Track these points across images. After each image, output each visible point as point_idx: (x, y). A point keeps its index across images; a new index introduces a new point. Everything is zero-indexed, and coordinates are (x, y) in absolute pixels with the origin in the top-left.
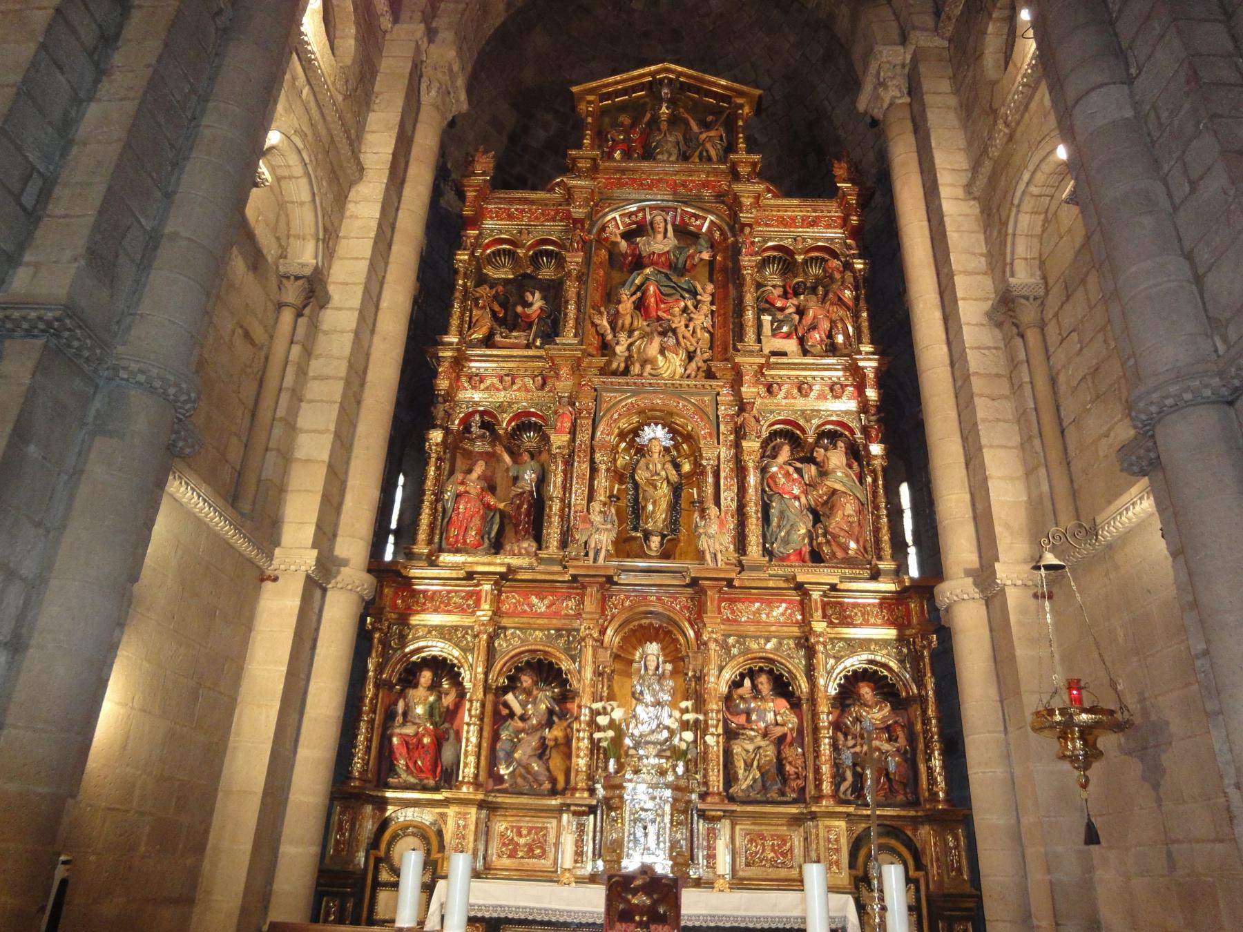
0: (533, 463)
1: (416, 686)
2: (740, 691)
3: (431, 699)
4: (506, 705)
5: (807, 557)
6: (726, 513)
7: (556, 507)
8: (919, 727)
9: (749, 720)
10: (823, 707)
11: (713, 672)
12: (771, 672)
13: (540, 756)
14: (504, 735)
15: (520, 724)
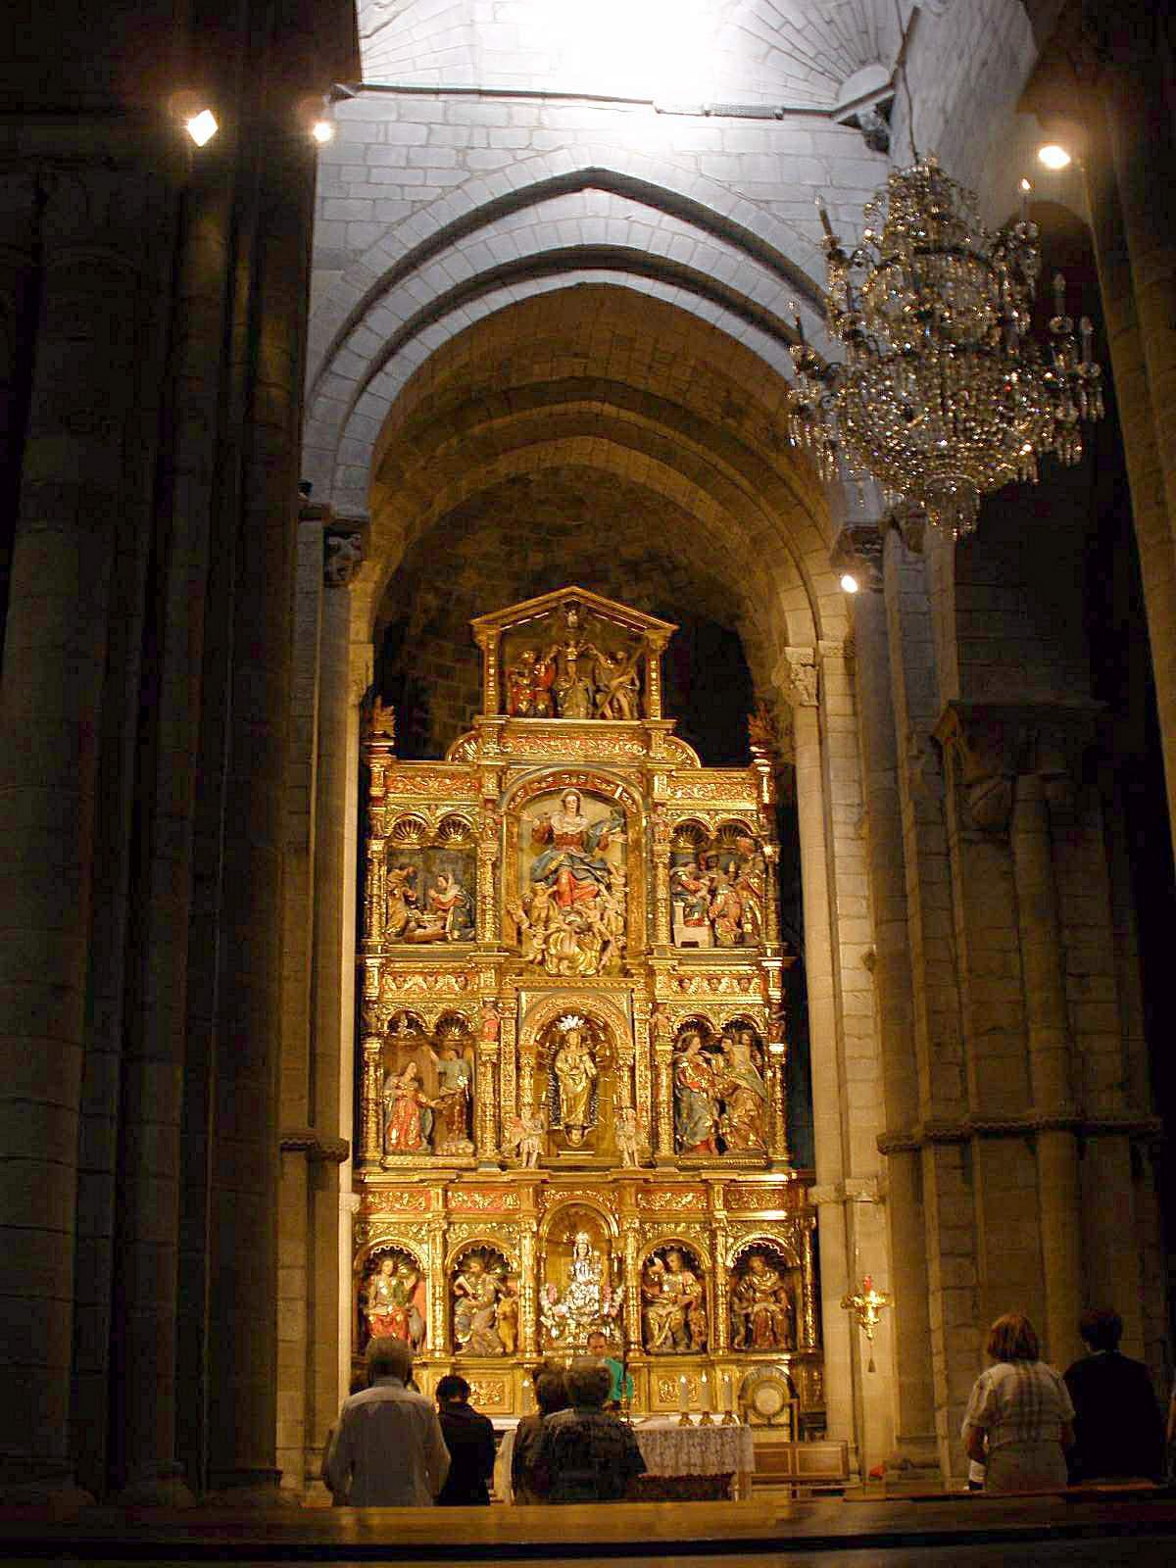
0: (460, 1062)
2: (655, 1268)
4: (460, 1287)
5: (713, 1145)
7: (490, 1111)
8: (799, 1291)
9: (661, 1291)
10: (722, 1278)
11: (630, 1251)
12: (680, 1250)
13: (492, 1326)
14: (459, 1310)
15: (473, 1302)
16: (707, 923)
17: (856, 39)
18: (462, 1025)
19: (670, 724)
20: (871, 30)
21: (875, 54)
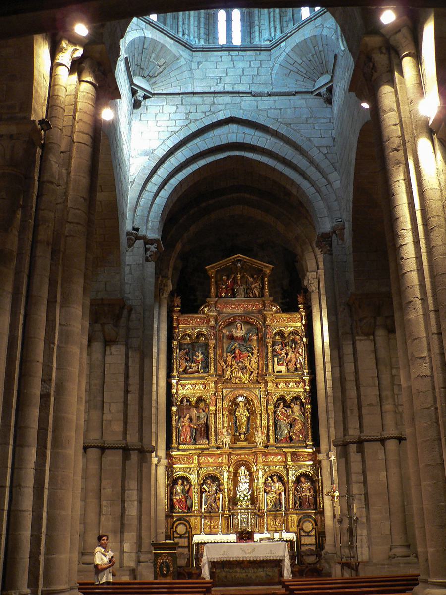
0: (204, 413)
1: (177, 484)
3: (182, 488)
4: (204, 489)
6: (264, 428)
7: (213, 430)
8: (317, 488)
9: (271, 489)
13: (214, 502)
15: (208, 494)
16: (285, 364)
17: (319, 66)
18: (204, 401)
19: (271, 299)
20: (324, 62)
21: (326, 70)
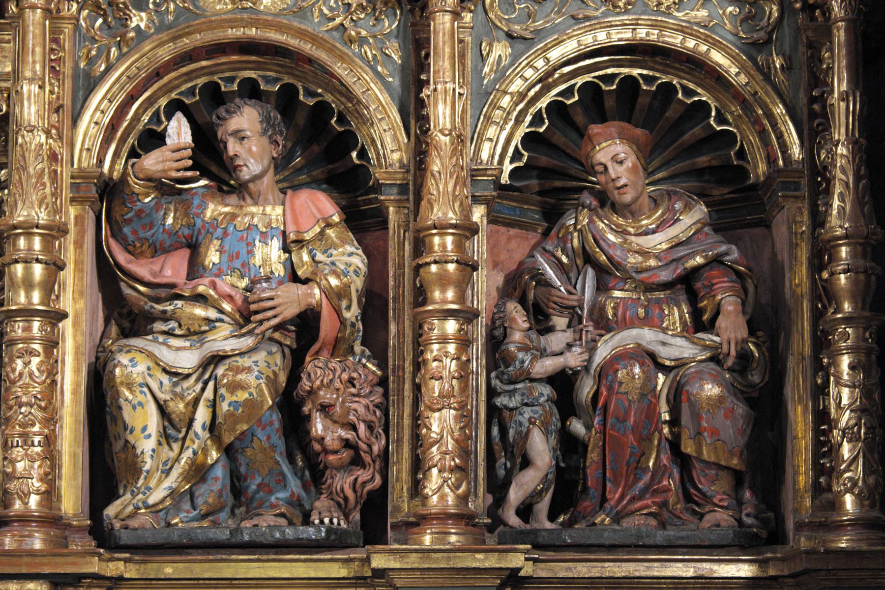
9: (195, 269)
